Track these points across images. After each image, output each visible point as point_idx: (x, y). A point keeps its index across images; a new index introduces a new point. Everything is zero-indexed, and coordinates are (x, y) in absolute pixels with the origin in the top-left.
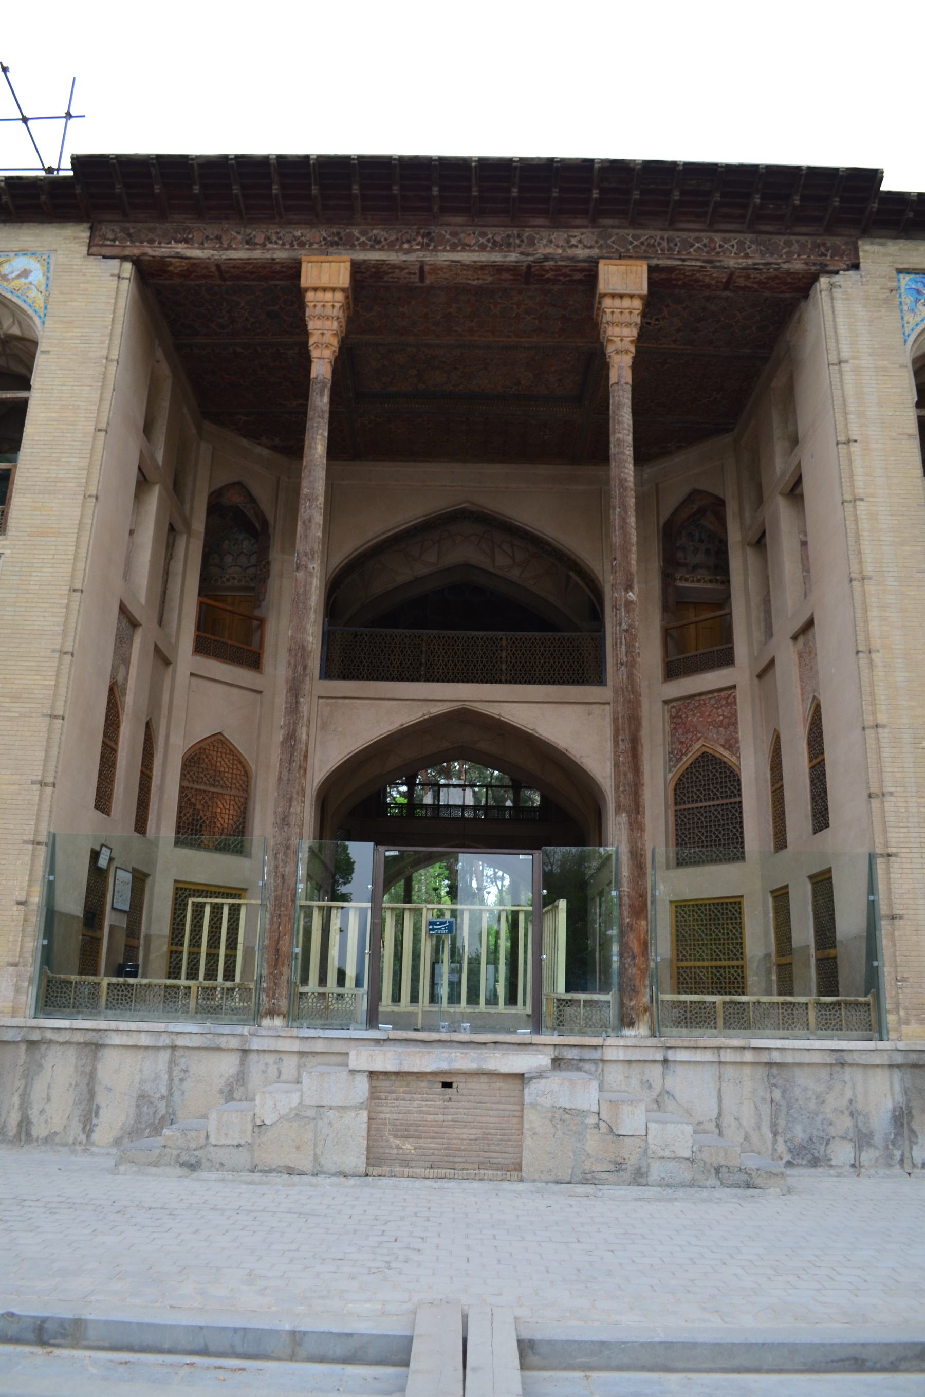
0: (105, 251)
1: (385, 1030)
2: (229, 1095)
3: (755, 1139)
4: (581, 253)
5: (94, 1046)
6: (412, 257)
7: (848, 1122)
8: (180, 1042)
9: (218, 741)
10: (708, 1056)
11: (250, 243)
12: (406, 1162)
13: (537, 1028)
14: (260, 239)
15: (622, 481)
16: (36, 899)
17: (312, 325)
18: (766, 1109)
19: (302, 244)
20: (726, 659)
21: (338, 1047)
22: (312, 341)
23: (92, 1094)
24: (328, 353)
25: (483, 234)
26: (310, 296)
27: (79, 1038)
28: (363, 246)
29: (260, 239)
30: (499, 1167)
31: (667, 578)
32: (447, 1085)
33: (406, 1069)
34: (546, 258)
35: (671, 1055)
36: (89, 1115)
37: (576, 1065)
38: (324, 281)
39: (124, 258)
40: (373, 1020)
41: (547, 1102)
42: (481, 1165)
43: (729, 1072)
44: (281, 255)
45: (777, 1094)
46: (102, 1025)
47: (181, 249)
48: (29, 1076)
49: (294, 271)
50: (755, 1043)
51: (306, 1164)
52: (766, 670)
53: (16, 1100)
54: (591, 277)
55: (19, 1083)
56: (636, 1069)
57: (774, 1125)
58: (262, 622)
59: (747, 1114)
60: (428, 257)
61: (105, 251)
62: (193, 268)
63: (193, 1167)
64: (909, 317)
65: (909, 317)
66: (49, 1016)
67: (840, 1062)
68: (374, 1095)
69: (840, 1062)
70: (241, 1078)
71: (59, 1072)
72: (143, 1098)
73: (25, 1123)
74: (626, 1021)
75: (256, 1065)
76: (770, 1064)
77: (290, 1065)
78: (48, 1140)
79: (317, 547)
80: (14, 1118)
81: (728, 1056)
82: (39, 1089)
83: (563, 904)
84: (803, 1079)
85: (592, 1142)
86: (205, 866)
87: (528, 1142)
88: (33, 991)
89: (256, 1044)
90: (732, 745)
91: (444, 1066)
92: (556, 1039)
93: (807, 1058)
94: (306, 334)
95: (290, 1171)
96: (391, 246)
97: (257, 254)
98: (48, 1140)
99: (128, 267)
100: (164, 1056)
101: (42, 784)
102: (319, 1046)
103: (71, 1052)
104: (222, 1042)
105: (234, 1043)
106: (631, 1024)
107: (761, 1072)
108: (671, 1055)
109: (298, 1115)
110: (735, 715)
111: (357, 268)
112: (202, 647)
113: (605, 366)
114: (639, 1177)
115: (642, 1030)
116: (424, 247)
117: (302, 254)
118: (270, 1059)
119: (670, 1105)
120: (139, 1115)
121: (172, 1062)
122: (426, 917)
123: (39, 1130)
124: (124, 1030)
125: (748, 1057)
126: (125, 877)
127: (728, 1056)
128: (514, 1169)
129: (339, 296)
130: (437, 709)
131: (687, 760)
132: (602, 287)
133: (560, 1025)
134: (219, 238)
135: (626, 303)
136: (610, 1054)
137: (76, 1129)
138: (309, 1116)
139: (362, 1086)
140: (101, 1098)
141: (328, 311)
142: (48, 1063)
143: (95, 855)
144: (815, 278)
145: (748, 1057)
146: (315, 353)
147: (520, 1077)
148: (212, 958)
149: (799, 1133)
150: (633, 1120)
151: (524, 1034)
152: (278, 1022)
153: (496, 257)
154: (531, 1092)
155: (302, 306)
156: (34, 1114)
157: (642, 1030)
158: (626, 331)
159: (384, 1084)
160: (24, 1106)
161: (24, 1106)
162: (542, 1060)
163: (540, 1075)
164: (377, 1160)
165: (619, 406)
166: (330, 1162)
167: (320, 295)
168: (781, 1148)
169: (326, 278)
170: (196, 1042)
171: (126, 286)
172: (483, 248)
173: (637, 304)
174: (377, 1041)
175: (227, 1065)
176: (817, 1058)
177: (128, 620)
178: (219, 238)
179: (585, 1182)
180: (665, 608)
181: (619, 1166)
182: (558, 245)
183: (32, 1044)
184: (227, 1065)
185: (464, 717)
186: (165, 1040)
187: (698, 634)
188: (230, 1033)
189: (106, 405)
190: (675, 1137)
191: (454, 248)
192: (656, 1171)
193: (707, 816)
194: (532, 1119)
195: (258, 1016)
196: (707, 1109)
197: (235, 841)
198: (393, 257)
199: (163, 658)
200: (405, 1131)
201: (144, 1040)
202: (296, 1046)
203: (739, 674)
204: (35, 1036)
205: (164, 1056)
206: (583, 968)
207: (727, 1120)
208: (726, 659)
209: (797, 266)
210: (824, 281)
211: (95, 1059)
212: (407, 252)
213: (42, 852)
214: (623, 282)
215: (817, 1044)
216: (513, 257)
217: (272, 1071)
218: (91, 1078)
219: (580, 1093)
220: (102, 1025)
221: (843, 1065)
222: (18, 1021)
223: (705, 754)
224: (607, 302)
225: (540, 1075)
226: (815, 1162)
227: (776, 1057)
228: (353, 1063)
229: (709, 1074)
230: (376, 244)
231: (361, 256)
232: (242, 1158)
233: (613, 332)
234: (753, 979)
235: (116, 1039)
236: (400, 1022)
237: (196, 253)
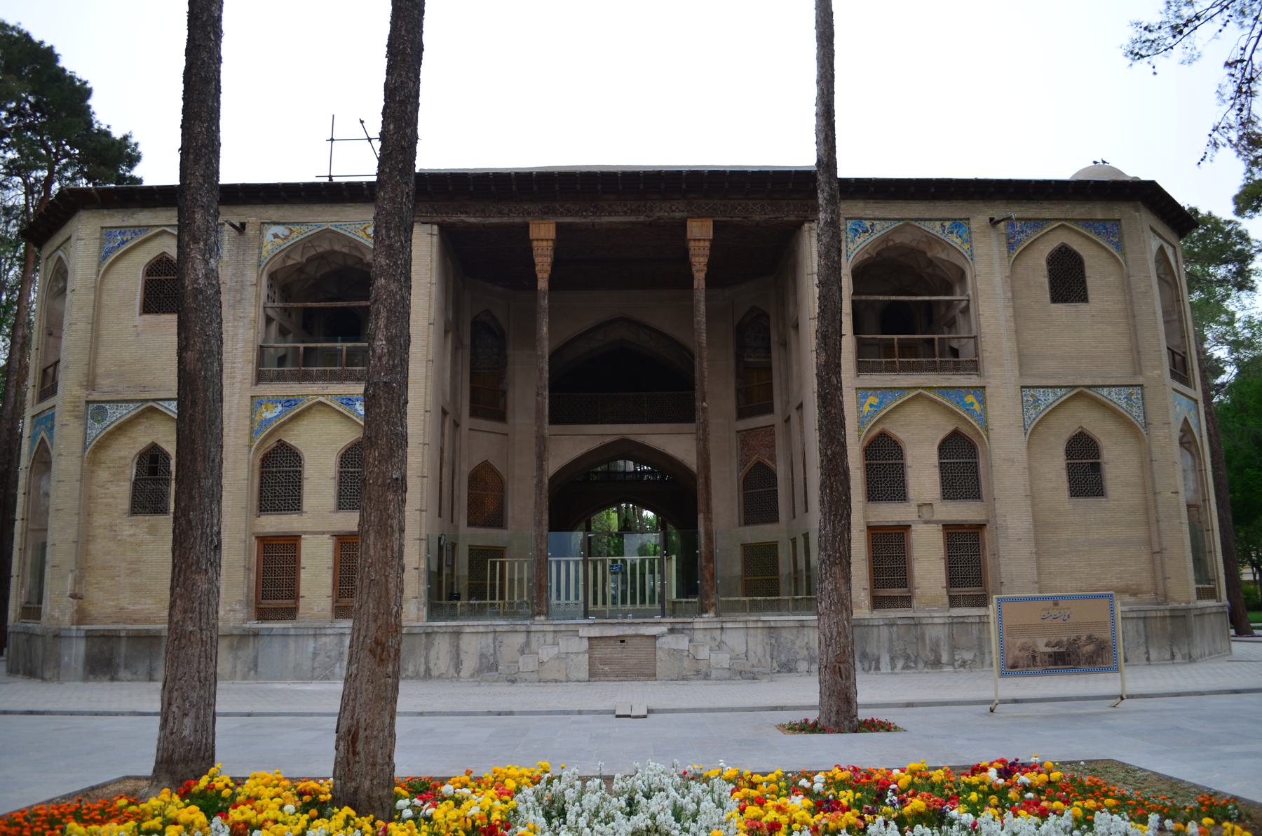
0: (422, 219)
1: (592, 619)
2: (522, 652)
3: (763, 660)
4: (678, 215)
5: (457, 634)
6: (588, 220)
7: (806, 652)
8: (498, 629)
9: (486, 465)
10: (741, 625)
11: (501, 213)
12: (606, 675)
13: (664, 616)
14: (506, 211)
15: (700, 343)
16: (423, 566)
17: (537, 260)
18: (768, 648)
19: (529, 214)
20: (769, 409)
21: (571, 628)
22: (537, 268)
23: (458, 655)
24: (546, 275)
25: (625, 205)
26: (535, 243)
27: (450, 630)
28: (562, 214)
29: (506, 211)
30: (646, 675)
31: (739, 357)
32: (622, 641)
33: (604, 634)
34: (659, 218)
35: (724, 625)
36: (458, 665)
37: (681, 631)
38: (542, 235)
39: (433, 223)
40: (586, 616)
41: (666, 647)
42: (639, 675)
43: (751, 632)
44: (518, 220)
45: (773, 641)
46: (461, 623)
47: (463, 217)
48: (428, 647)
49: (526, 227)
50: (763, 618)
51: (563, 678)
52: (788, 420)
53: (423, 660)
54: (683, 225)
55: (424, 652)
56: (708, 632)
57: (771, 655)
58: (504, 393)
59: (759, 649)
60: (597, 220)
61: (422, 219)
62: (471, 225)
63: (513, 681)
64: (851, 245)
65: (851, 245)
66: (434, 620)
67: (802, 626)
68: (590, 647)
69: (802, 626)
70: (527, 644)
71: (442, 646)
72: (482, 656)
73: (428, 670)
74: (703, 610)
75: (534, 638)
76: (770, 628)
77: (550, 637)
78: (440, 677)
79: (547, 383)
80: (422, 668)
81: (751, 625)
82: (433, 654)
83: (674, 557)
84: (785, 634)
85: (686, 663)
86: (486, 536)
87: (658, 664)
88: (425, 609)
89: (533, 628)
90: (773, 458)
91: (621, 633)
92: (672, 620)
93: (787, 624)
94: (533, 265)
95: (556, 681)
96: (576, 214)
97: (505, 220)
98: (440, 677)
99: (435, 227)
100: (491, 636)
101: (421, 511)
102: (563, 628)
103: (447, 637)
104: (518, 628)
105: (523, 628)
106: (706, 612)
107: (766, 631)
108: (724, 625)
109: (558, 657)
110: (774, 441)
111: (560, 228)
112: (474, 413)
113: (692, 278)
114: (707, 677)
115: (712, 614)
116: (594, 214)
117: (528, 219)
118: (540, 635)
119: (724, 647)
120: (481, 663)
121: (495, 639)
122: (609, 563)
123: (435, 673)
124: (471, 625)
125: (760, 625)
126: (449, 547)
127: (751, 625)
128: (653, 676)
129: (550, 243)
130: (608, 440)
131: (750, 465)
132: (689, 236)
133: (674, 613)
134: (484, 211)
135: (702, 243)
136: (696, 626)
137: (452, 671)
138: (563, 657)
139: (586, 643)
140: (462, 657)
141: (546, 252)
142: (436, 642)
143: (440, 539)
144: (802, 224)
145: (760, 625)
146: (539, 276)
147: (654, 636)
148: (493, 586)
149: (783, 658)
150: (703, 653)
151: (658, 618)
152: (543, 618)
153: (633, 219)
154: (659, 643)
155: (531, 249)
156: (431, 665)
157: (712, 614)
158: (702, 259)
159: (595, 642)
160: (427, 663)
161: (427, 663)
162: (664, 629)
163: (663, 635)
164: (593, 675)
165: (699, 301)
166: (573, 676)
167: (540, 243)
168: (775, 664)
169: (543, 234)
170: (505, 629)
171: (435, 239)
172: (625, 213)
173: (707, 244)
174: (590, 625)
175: (520, 639)
176: (791, 624)
177: (444, 413)
178: (484, 211)
179: (683, 679)
180: (738, 375)
181: (698, 672)
182: (664, 211)
183: (428, 634)
184: (520, 639)
186: (491, 629)
187: (756, 392)
188: (521, 624)
189: (433, 310)
190: (723, 659)
191: (610, 215)
192: (714, 674)
193: (760, 498)
194: (659, 653)
195: (533, 616)
196: (741, 648)
197: (497, 520)
198: (577, 220)
199: (456, 425)
200: (605, 662)
201: (481, 629)
202: (552, 628)
203: (775, 419)
204: (429, 630)
205: (491, 636)
206: (689, 585)
207: (751, 653)
208: (769, 409)
209: (793, 218)
210: (806, 225)
211: (458, 639)
212: (585, 217)
213: (424, 544)
214: (700, 232)
215: (792, 618)
216: (642, 218)
217: (542, 640)
218: (457, 648)
219: (682, 642)
220: (461, 623)
221: (803, 627)
222: (420, 624)
223: (759, 463)
224: (692, 244)
225: (663, 635)
226: (790, 671)
227: (773, 624)
228: (581, 634)
229: (742, 632)
230: (569, 213)
231: (561, 220)
232: (535, 676)
233: (694, 260)
234: (783, 587)
235: (468, 630)
236: (600, 615)
237: (472, 220)
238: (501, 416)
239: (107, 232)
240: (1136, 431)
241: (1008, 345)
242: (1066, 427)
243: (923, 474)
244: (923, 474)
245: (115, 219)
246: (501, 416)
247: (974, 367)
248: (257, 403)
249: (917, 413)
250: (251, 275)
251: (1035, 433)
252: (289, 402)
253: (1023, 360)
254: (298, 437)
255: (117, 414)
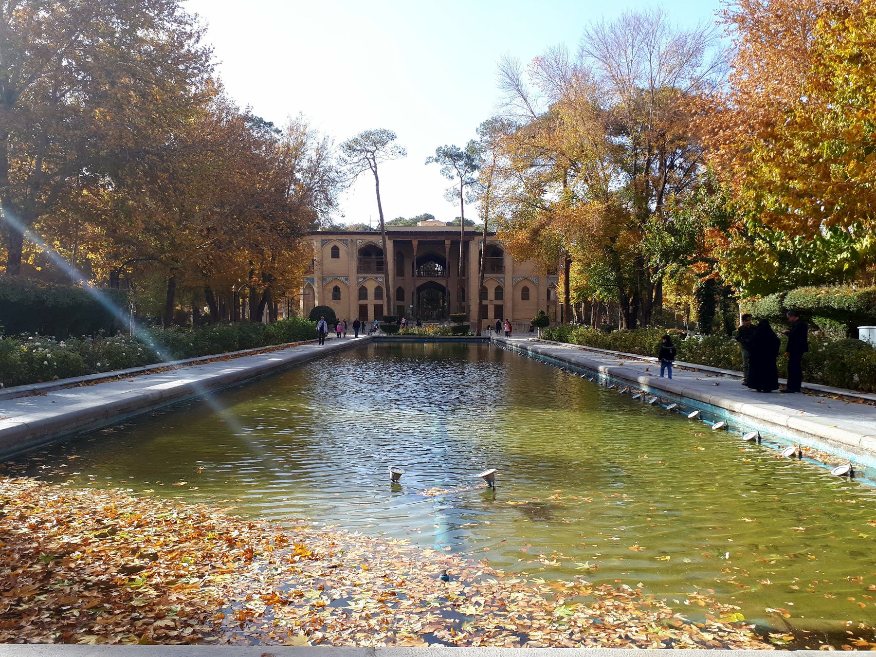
169: (415, 242)
185: (431, 282)
238: (403, 276)
239: (323, 240)
240: (537, 287)
241: (511, 268)
242: (522, 285)
243: (491, 295)
244: (491, 295)
245: (324, 237)
246: (403, 276)
247: (503, 273)
248: (358, 278)
249: (491, 282)
250: (355, 251)
251: (514, 287)
252: (364, 278)
253: (513, 271)
254: (366, 285)
255: (329, 279)
